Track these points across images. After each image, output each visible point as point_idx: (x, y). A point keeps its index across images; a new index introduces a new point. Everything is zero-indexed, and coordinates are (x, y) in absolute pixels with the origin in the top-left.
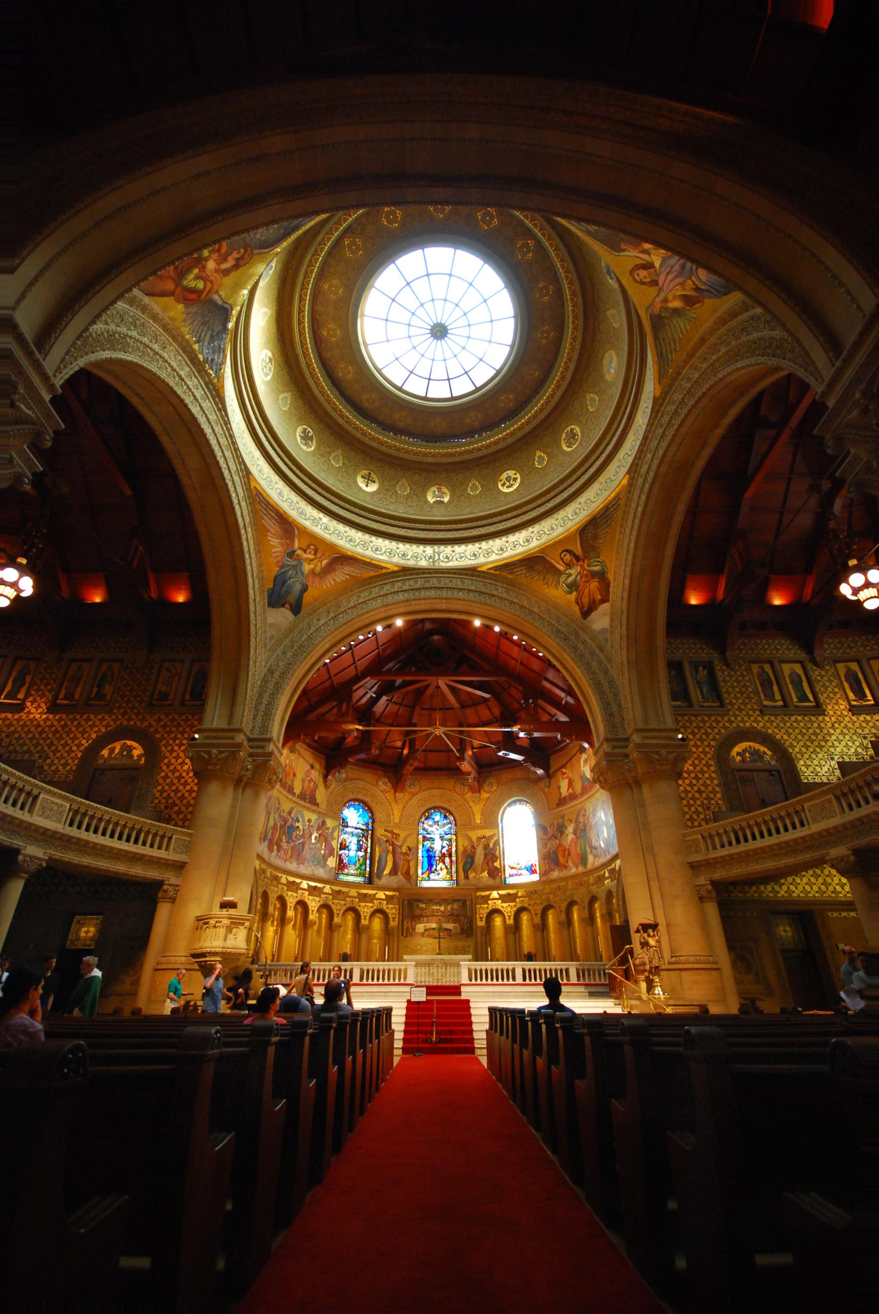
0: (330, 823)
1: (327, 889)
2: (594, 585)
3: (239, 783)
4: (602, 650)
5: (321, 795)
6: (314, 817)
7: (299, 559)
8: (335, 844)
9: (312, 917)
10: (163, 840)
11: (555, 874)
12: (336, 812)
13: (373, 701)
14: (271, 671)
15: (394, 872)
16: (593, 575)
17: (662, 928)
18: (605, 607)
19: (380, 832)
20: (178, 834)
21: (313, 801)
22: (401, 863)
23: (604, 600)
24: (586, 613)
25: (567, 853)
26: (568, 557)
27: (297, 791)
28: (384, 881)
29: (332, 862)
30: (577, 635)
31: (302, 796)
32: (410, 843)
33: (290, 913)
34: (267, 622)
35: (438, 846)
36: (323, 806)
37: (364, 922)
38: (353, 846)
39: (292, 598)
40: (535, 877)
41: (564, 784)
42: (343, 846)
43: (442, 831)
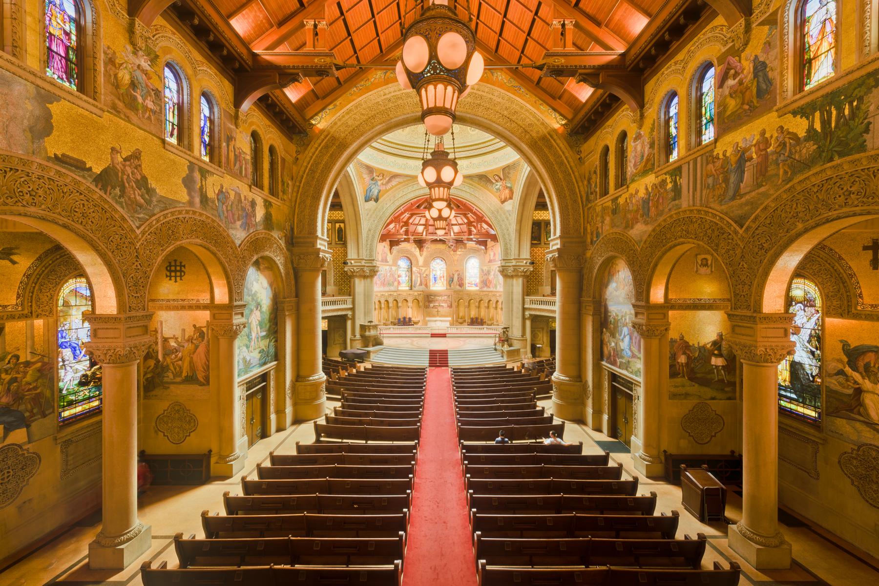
0: (394, 268)
1: (395, 294)
2: (507, 191)
3: (365, 277)
4: (507, 219)
5: (390, 258)
6: (387, 267)
7: (376, 180)
9: (391, 305)
10: (345, 302)
11: (485, 289)
12: (395, 264)
13: (409, 218)
14: (370, 230)
15: (421, 284)
16: (507, 187)
18: (510, 201)
19: (414, 269)
20: (349, 299)
21: (387, 261)
23: (511, 198)
24: (503, 202)
25: (490, 282)
26: (497, 178)
29: (396, 284)
30: (498, 212)
32: (427, 273)
33: (383, 306)
34: (365, 208)
35: (439, 273)
36: (391, 263)
39: (374, 197)
40: (477, 288)
41: (492, 254)
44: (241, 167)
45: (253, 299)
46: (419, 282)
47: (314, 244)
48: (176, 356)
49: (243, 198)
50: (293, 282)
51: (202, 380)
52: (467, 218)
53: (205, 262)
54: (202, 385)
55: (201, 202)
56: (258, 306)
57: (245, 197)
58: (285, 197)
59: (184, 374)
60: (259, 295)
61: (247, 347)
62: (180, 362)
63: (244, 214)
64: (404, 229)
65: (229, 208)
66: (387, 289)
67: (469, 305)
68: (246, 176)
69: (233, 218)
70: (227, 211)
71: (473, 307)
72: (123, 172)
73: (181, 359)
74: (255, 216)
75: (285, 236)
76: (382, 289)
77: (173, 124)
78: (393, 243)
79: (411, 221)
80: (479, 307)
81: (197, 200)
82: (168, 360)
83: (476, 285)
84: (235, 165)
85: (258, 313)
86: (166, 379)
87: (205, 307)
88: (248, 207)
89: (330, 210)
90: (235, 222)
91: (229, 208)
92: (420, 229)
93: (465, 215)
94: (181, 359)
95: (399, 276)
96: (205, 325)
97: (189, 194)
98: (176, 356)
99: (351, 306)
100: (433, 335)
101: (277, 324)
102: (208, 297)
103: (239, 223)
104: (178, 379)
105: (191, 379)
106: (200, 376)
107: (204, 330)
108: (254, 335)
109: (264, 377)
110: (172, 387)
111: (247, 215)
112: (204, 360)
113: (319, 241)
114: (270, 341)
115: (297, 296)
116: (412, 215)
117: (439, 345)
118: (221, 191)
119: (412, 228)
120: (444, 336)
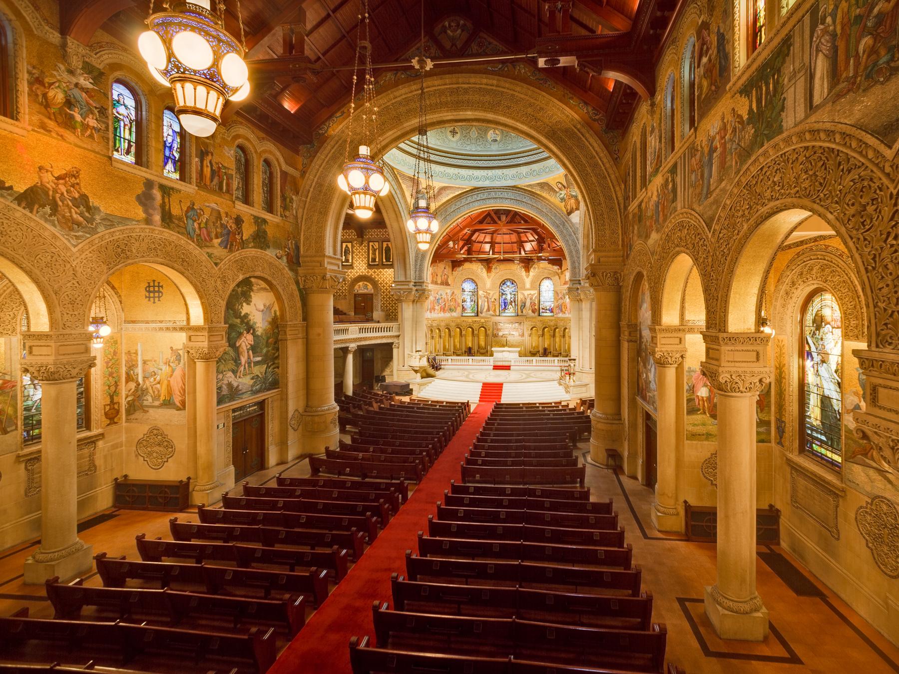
8: (460, 301)
11: (560, 315)
13: (472, 235)
15: (488, 310)
17: (577, 361)
19: (480, 293)
22: (491, 306)
27: (439, 282)
28: (484, 314)
29: (459, 309)
31: (442, 284)
35: (509, 297)
37: (476, 332)
38: (469, 300)
42: (464, 301)
43: (510, 290)
44: (221, 183)
45: (242, 322)
46: (486, 308)
47: (321, 264)
48: (155, 379)
49: (223, 215)
50: (299, 304)
51: (179, 404)
52: (537, 233)
53: (179, 285)
54: (179, 409)
55: (163, 219)
56: (250, 328)
57: (227, 214)
58: (287, 213)
59: (162, 398)
60: (251, 317)
61: (234, 372)
62: (158, 386)
63: (225, 232)
64: (466, 248)
65: (203, 225)
66: (448, 315)
67: (543, 335)
68: (228, 191)
69: (209, 235)
70: (200, 228)
71: (547, 336)
72: (55, 191)
73: (159, 383)
74: (241, 233)
75: (288, 255)
76: (442, 315)
77: (129, 141)
78: (456, 264)
79: (474, 238)
80: (554, 336)
81: (157, 218)
82: (147, 382)
83: (552, 311)
84: (212, 181)
85: (250, 337)
86: (145, 403)
87: (182, 329)
88: (231, 225)
89: (344, 229)
90: (211, 240)
91: (203, 225)
92: (487, 247)
93: (534, 230)
94: (159, 383)
95: (464, 301)
96: (181, 347)
97: (146, 211)
98: (155, 379)
99: (397, 334)
100: (496, 368)
101: (278, 350)
102: (185, 318)
103: (216, 242)
104: (157, 403)
105: (168, 403)
106: (177, 400)
107: (181, 352)
108: (243, 360)
109: (261, 404)
110: (151, 411)
111: (229, 233)
112: (181, 384)
113: (326, 260)
114: (268, 367)
115: (305, 319)
116: (474, 232)
117: (494, 377)
118: (191, 208)
119: (476, 247)
120: (508, 368)
